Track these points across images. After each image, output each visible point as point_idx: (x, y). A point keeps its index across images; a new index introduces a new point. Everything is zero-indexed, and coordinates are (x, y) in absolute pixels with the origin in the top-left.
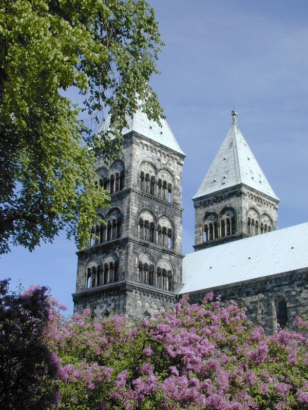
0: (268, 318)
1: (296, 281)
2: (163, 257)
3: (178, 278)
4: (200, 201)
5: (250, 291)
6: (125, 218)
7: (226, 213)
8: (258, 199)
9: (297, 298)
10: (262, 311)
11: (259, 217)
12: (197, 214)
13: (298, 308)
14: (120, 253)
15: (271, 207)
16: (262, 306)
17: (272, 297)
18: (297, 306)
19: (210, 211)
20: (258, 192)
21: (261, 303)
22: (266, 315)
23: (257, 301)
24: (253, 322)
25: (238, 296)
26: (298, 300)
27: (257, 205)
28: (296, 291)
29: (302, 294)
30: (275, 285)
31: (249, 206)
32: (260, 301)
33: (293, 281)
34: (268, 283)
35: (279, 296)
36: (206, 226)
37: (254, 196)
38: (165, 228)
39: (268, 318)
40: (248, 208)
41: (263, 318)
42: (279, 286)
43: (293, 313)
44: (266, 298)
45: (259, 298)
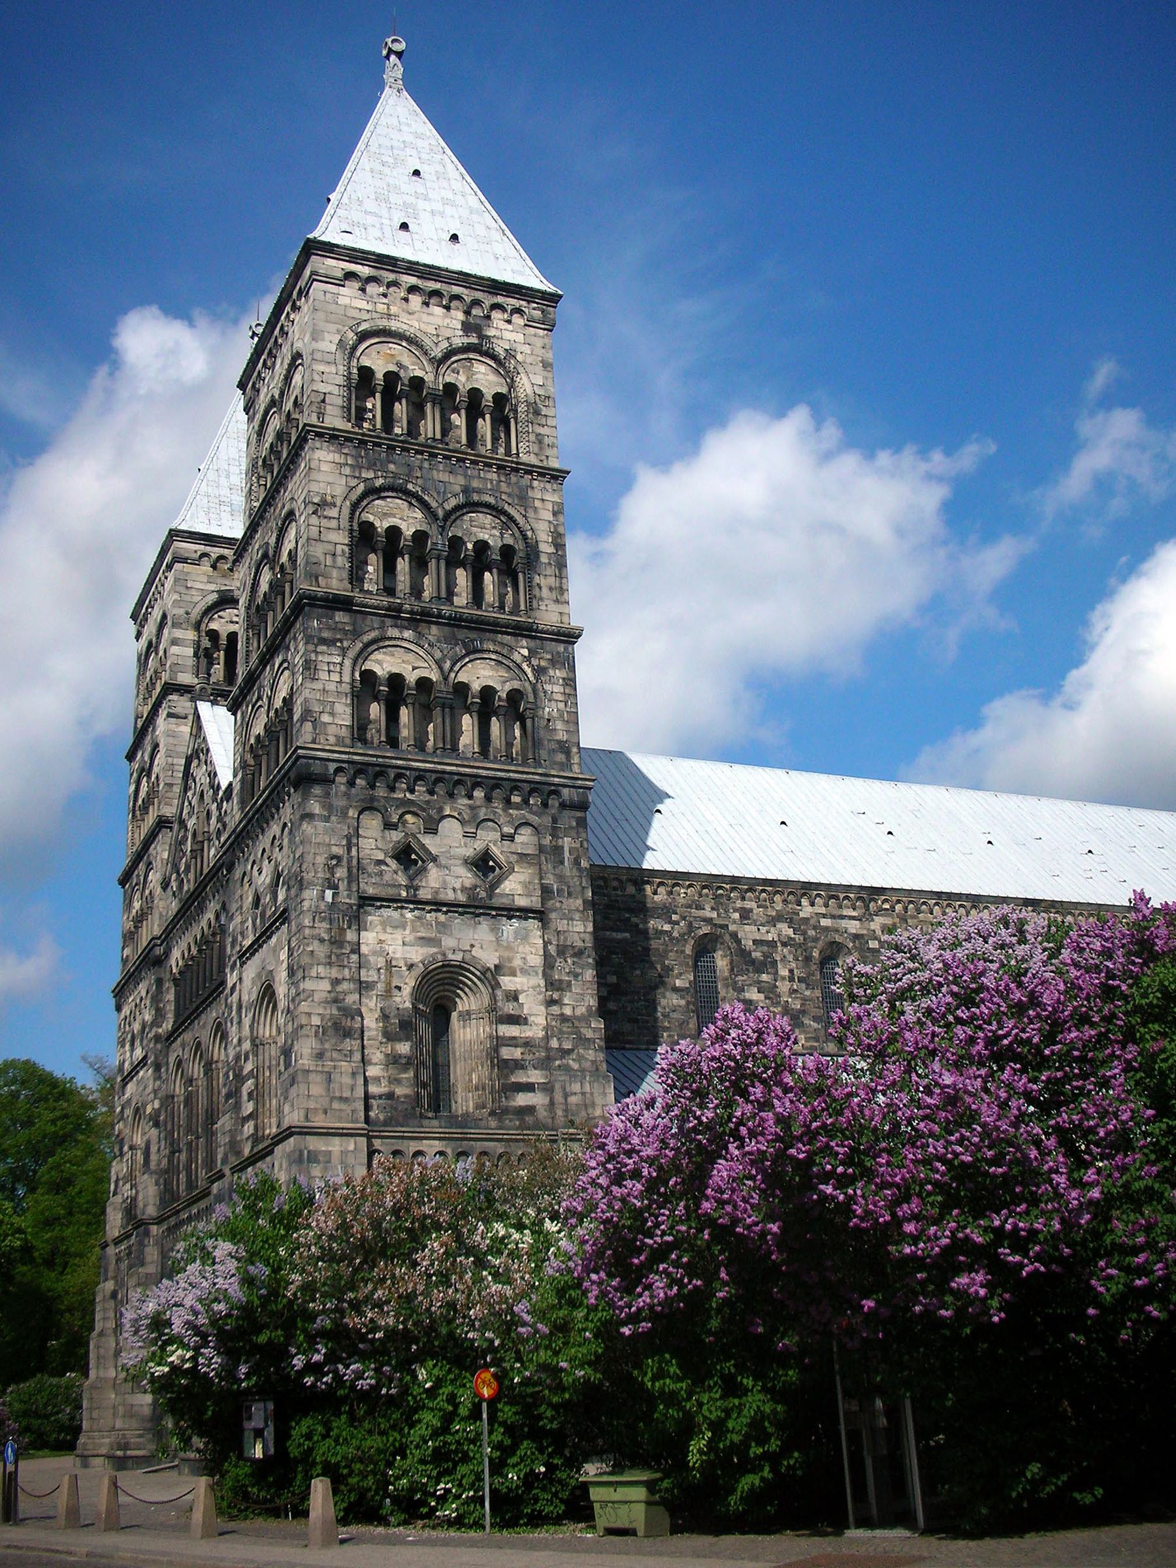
0: (808, 993)
5: (751, 910)
6: (544, 559)
10: (791, 971)
14: (539, 671)
16: (790, 958)
17: (816, 940)
24: (766, 998)
25: (714, 915)
28: (880, 941)
30: (823, 910)
32: (784, 944)
34: (805, 902)
39: (808, 993)
42: (833, 917)
44: (799, 938)
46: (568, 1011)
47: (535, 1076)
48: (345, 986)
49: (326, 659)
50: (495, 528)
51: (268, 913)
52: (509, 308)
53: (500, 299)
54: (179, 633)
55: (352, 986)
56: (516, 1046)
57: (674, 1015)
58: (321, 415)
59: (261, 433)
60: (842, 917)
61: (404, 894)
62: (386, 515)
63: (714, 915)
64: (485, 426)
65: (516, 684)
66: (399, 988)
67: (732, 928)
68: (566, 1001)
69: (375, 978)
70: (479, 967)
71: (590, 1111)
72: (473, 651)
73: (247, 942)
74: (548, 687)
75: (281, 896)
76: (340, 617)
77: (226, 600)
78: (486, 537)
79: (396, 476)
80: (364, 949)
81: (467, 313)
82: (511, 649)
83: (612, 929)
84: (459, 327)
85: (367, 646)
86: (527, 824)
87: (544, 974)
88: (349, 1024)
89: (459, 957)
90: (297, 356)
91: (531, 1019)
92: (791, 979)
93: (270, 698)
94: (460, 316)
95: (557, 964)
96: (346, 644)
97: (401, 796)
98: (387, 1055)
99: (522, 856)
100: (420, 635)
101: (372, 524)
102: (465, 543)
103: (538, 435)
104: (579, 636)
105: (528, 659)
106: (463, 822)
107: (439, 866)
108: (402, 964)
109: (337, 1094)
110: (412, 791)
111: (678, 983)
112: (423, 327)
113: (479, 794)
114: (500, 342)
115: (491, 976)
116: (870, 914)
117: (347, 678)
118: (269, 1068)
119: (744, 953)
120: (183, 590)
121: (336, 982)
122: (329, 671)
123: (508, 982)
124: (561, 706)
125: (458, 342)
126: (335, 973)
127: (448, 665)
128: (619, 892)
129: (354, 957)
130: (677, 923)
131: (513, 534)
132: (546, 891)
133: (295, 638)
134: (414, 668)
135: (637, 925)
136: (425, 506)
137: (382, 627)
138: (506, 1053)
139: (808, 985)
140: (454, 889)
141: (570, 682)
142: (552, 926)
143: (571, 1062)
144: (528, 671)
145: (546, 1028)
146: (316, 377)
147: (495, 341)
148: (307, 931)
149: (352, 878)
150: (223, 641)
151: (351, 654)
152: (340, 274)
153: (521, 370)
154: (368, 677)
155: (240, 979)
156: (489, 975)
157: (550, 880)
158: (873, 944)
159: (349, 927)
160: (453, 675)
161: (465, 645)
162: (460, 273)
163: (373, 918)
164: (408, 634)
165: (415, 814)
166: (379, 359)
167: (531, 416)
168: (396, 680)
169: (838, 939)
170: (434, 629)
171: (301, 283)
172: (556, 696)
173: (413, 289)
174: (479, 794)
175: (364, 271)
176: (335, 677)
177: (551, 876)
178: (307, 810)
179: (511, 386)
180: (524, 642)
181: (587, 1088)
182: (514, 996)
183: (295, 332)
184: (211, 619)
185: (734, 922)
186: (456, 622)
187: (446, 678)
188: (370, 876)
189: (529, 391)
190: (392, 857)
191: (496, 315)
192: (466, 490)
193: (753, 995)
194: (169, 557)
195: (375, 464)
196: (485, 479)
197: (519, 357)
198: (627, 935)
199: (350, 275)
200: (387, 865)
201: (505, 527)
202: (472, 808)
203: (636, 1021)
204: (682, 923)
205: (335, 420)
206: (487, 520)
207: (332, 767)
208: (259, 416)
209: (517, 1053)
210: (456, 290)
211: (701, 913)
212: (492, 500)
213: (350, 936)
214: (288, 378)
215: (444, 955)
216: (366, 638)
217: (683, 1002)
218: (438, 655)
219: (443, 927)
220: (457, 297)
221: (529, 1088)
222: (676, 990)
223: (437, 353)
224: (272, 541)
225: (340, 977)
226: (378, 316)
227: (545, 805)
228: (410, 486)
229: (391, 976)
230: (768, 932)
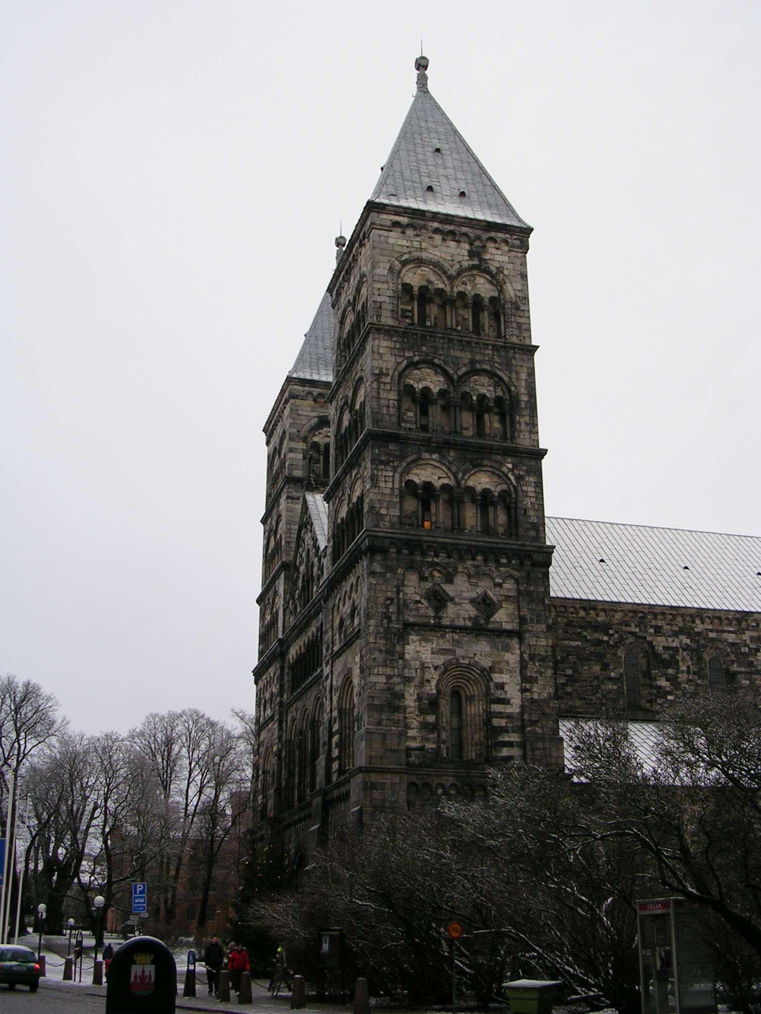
0: (699, 682)
5: (662, 627)
6: (523, 405)
9: (751, 659)
10: (688, 667)
18: (751, 673)
24: (671, 684)
25: (637, 630)
26: (752, 661)
30: (710, 627)
32: (684, 649)
34: (698, 622)
42: (717, 631)
45: (681, 643)
46: (536, 696)
47: (514, 737)
48: (395, 679)
49: (384, 473)
50: (490, 385)
51: (349, 632)
52: (498, 240)
53: (493, 234)
54: (293, 445)
55: (399, 680)
56: (502, 718)
58: (379, 316)
59: (342, 322)
60: (724, 631)
61: (432, 622)
62: (420, 380)
63: (637, 630)
64: (486, 318)
65: (504, 487)
66: (429, 681)
67: (649, 639)
68: (535, 690)
69: (414, 675)
70: (479, 668)
71: (549, 759)
72: (477, 466)
73: (336, 649)
74: (525, 488)
75: (356, 622)
76: (391, 446)
77: (323, 422)
78: (485, 391)
79: (427, 354)
80: (407, 656)
81: (471, 244)
82: (501, 464)
83: (570, 640)
84: (466, 254)
85: (409, 464)
86: (511, 576)
87: (521, 672)
88: (397, 704)
89: (466, 661)
90: (363, 276)
91: (512, 701)
92: (688, 672)
93: (349, 496)
94: (467, 247)
95: (529, 666)
96: (396, 464)
97: (431, 560)
98: (421, 723)
99: (507, 598)
100: (443, 456)
101: (412, 386)
102: (471, 397)
103: (518, 323)
104: (546, 454)
105: (512, 470)
106: (469, 576)
107: (455, 604)
108: (431, 666)
109: (389, 747)
110: (437, 556)
111: (612, 675)
112: (443, 255)
113: (480, 558)
114: (493, 263)
115: (487, 673)
116: (743, 630)
117: (397, 486)
118: (349, 728)
119: (657, 656)
120: (296, 416)
121: (389, 677)
122: (386, 481)
123: (497, 678)
124: (533, 500)
125: (466, 264)
126: (389, 671)
127: (460, 475)
128: (574, 616)
129: (400, 661)
130: (612, 635)
131: (502, 390)
132: (522, 620)
133: (364, 459)
134: (439, 478)
135: (586, 637)
136: (445, 373)
137: (419, 452)
138: (496, 722)
140: (464, 619)
141: (539, 485)
142: (526, 641)
143: (537, 729)
144: (512, 478)
145: (522, 707)
146: (376, 292)
147: (490, 262)
148: (372, 645)
149: (399, 612)
150: (322, 449)
151: (399, 470)
152: (389, 223)
153: (507, 280)
154: (410, 483)
155: (332, 671)
156: (486, 673)
157: (525, 612)
159: (398, 643)
160: (464, 482)
161: (471, 461)
162: (466, 218)
163: (413, 637)
164: (434, 456)
165: (439, 571)
166: (414, 278)
167: (513, 311)
168: (428, 486)
170: (452, 453)
171: (365, 229)
172: (530, 494)
173: (437, 231)
174: (480, 558)
175: (404, 220)
176: (390, 485)
177: (525, 610)
178: (372, 569)
179: (501, 291)
180: (510, 460)
181: (547, 745)
182: (501, 686)
183: (362, 260)
184: (314, 435)
185: (650, 634)
186: (464, 447)
187: (458, 483)
188: (411, 610)
189: (512, 295)
190: (424, 598)
191: (490, 245)
192: (472, 362)
193: (663, 683)
194: (286, 395)
195: (413, 347)
196: (484, 354)
197: (506, 272)
198: (580, 643)
199: (396, 224)
200: (422, 604)
201: (496, 385)
202: (476, 567)
203: (585, 699)
204: (616, 636)
205: (387, 320)
206: (485, 380)
207: (388, 541)
208: (340, 312)
209: (503, 723)
210: (464, 229)
211: (628, 629)
212: (488, 368)
213: (398, 648)
214: (358, 290)
215: (458, 660)
216: (409, 460)
217: (615, 687)
218: (454, 469)
219: (457, 643)
220: (466, 234)
221: (510, 744)
222: (610, 679)
223: (453, 272)
224: (350, 395)
225: (392, 673)
226: (414, 249)
227: (522, 564)
228: (436, 361)
229: (424, 674)
230: (673, 641)
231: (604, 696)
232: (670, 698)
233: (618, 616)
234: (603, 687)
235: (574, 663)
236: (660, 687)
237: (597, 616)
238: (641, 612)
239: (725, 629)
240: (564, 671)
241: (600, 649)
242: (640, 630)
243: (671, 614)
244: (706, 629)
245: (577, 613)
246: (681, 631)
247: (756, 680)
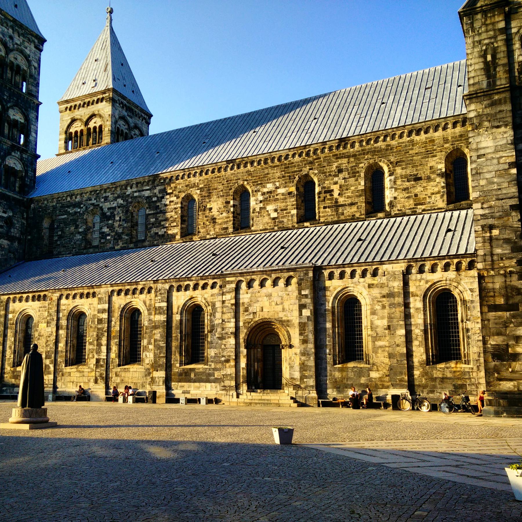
0: (125, 225)
1: (158, 185)
2: (13, 154)
3: (31, 180)
4: (66, 106)
5: (108, 196)
7: (93, 121)
8: (129, 109)
10: (120, 218)
11: (130, 129)
12: (62, 120)
13: (158, 215)
15: (142, 120)
16: (121, 212)
17: (131, 202)
19: (76, 117)
20: (129, 101)
21: (119, 209)
22: (124, 222)
23: (115, 207)
25: (95, 201)
27: (128, 115)
28: (158, 197)
29: (163, 200)
30: (135, 189)
31: (119, 115)
32: (119, 207)
33: (155, 186)
35: (139, 202)
36: (71, 133)
37: (125, 104)
38: (16, 121)
39: (125, 225)
40: (117, 117)
41: (121, 225)
42: (139, 191)
43: (153, 220)
44: (125, 203)
45: (118, 204)
57: (78, 242)
67: (101, 205)
111: (80, 230)
116: (155, 186)
130: (82, 208)
139: (126, 222)
158: (155, 199)
169: (140, 200)
193: (106, 230)
198: (66, 216)
211: (91, 202)
217: (81, 237)
222: (79, 233)
231: (75, 243)
232: (108, 238)
233: (86, 197)
234: (75, 238)
235: (63, 227)
236: (104, 232)
237: (76, 198)
238: (97, 190)
239: (144, 188)
240: (57, 233)
241: (75, 217)
242: (97, 201)
243: (113, 187)
244: (133, 192)
245: (67, 199)
246: (119, 197)
247: (159, 217)
